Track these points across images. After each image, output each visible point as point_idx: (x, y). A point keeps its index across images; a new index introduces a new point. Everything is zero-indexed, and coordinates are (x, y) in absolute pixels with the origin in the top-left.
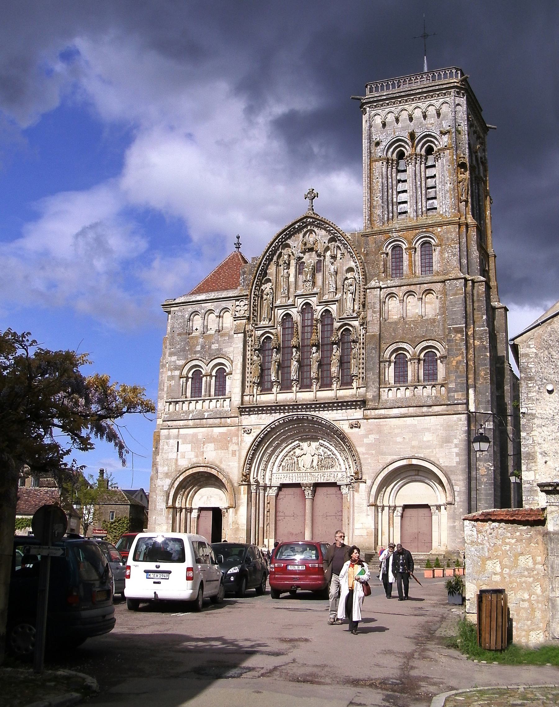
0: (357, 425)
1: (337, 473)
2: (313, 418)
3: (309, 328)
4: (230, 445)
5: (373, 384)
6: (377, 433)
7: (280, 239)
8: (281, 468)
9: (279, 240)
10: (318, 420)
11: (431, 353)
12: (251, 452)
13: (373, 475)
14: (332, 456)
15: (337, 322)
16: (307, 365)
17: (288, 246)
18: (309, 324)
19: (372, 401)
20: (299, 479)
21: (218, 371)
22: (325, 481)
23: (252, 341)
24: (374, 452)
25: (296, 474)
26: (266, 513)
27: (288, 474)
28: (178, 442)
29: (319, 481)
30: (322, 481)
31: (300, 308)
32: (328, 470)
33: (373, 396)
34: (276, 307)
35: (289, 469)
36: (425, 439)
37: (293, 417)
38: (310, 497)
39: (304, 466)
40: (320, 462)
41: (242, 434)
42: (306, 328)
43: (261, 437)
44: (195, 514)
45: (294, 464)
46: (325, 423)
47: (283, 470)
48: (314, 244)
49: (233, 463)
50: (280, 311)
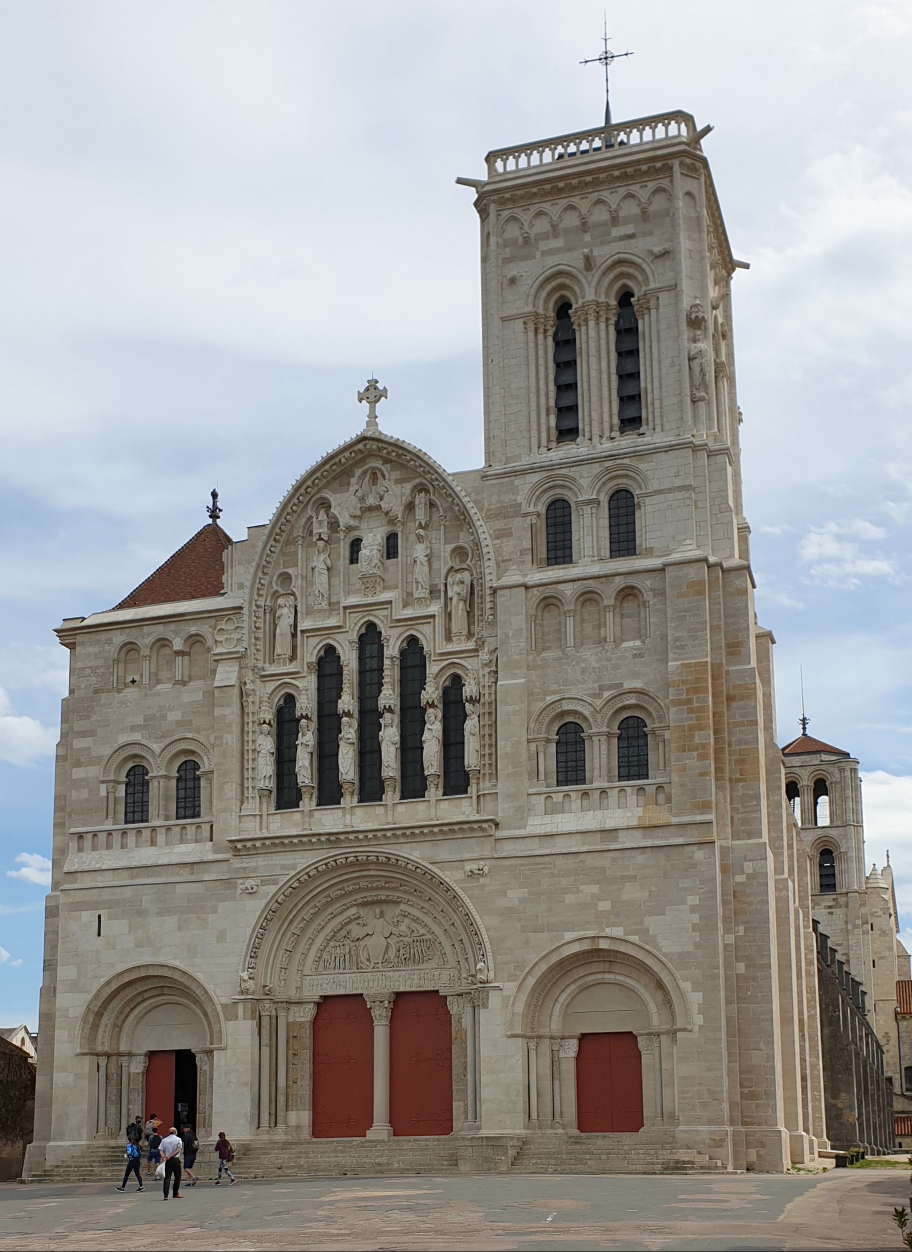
0: (481, 872)
2: (389, 859)
3: (375, 674)
7: (308, 487)
9: (306, 489)
11: (631, 722)
15: (434, 661)
16: (372, 752)
17: (326, 505)
18: (375, 666)
21: (183, 768)
22: (414, 989)
23: (253, 702)
26: (290, 1058)
28: (99, 916)
29: (402, 989)
30: (408, 989)
31: (355, 633)
32: (421, 966)
34: (302, 632)
35: (338, 965)
36: (625, 897)
38: (383, 1023)
39: (369, 960)
40: (402, 952)
42: (368, 674)
44: (137, 1066)
45: (347, 956)
46: (413, 868)
47: (325, 968)
48: (381, 498)
50: (313, 641)
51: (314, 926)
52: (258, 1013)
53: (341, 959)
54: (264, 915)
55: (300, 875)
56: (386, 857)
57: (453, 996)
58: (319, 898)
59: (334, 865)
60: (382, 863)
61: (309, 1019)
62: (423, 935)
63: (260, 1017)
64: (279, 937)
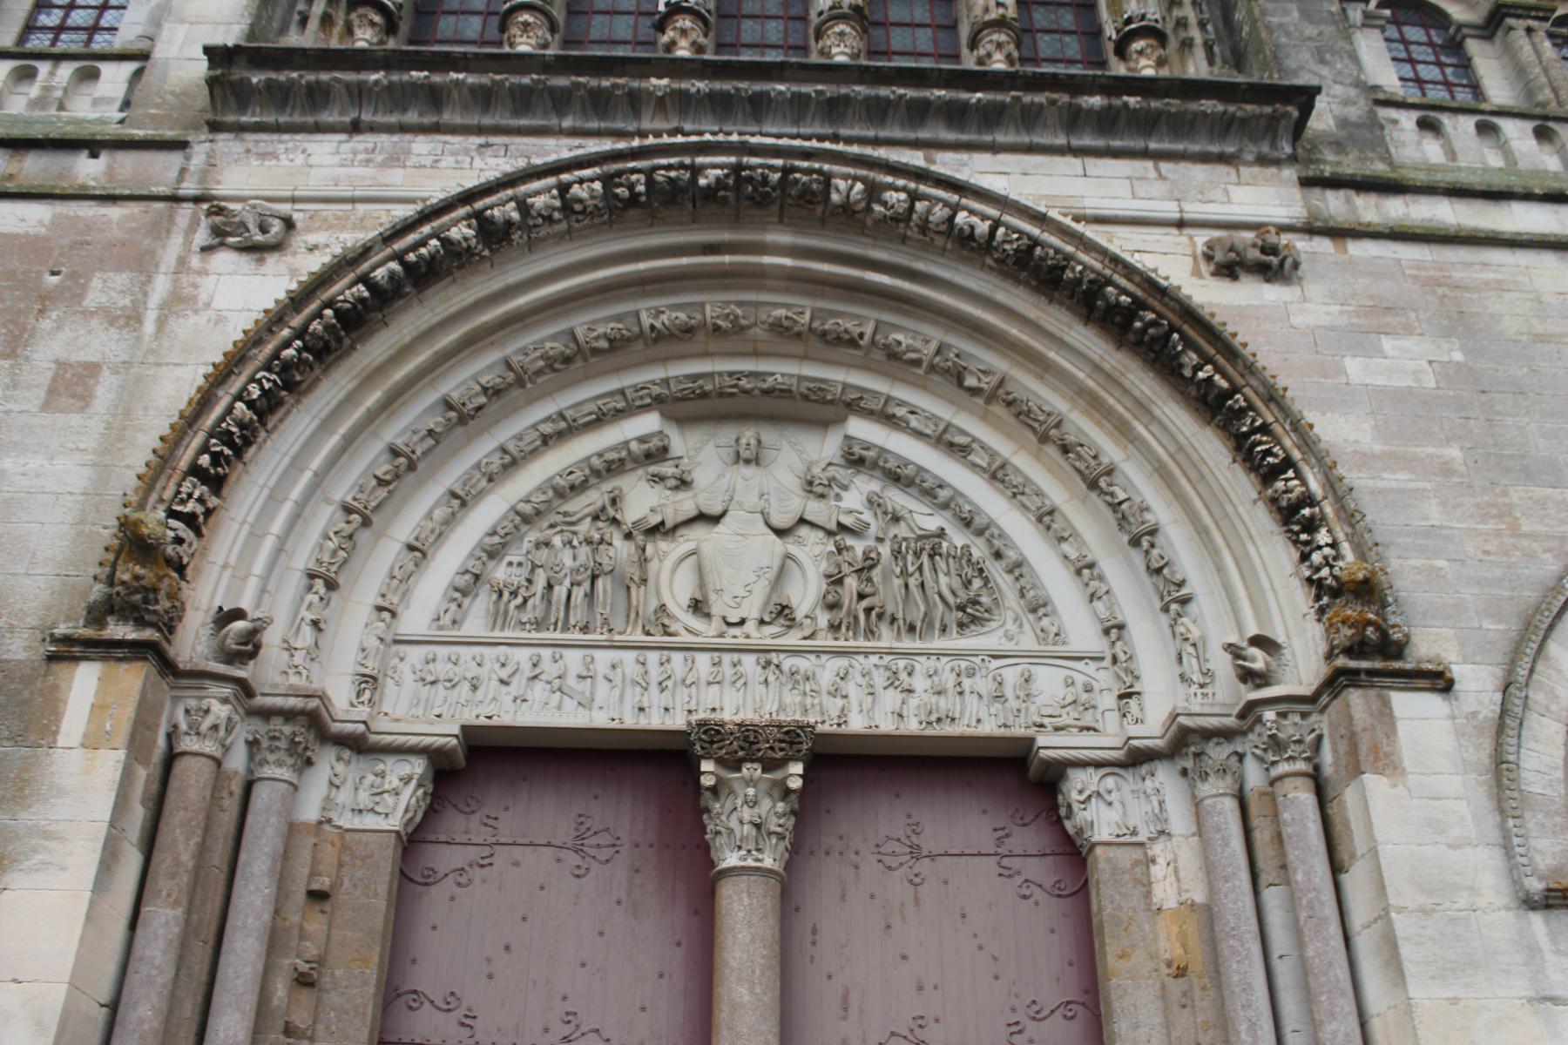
0: (1274, 260)
1: (1023, 666)
4: (46, 324)
5: (1322, 62)
6: (1446, 333)
8: (481, 604)
10: (920, 206)
12: (252, 380)
13: (1500, 630)
14: (958, 538)
19: (1339, 146)
20: (655, 698)
22: (912, 726)
24: (1454, 453)
25: (630, 656)
27: (546, 653)
29: (856, 724)
33: (1343, 123)
37: (696, 171)
39: (698, 606)
40: (852, 583)
41: (195, 261)
43: (380, 274)
46: (983, 227)
47: (499, 617)
49: (35, 462)
51: (483, 449)
52: (161, 742)
53: (579, 594)
54: (297, 321)
55: (488, 201)
56: (863, 180)
57: (1098, 764)
58: (527, 339)
59: (641, 188)
60: (846, 208)
61: (395, 822)
62: (941, 533)
63: (171, 758)
64: (334, 441)
